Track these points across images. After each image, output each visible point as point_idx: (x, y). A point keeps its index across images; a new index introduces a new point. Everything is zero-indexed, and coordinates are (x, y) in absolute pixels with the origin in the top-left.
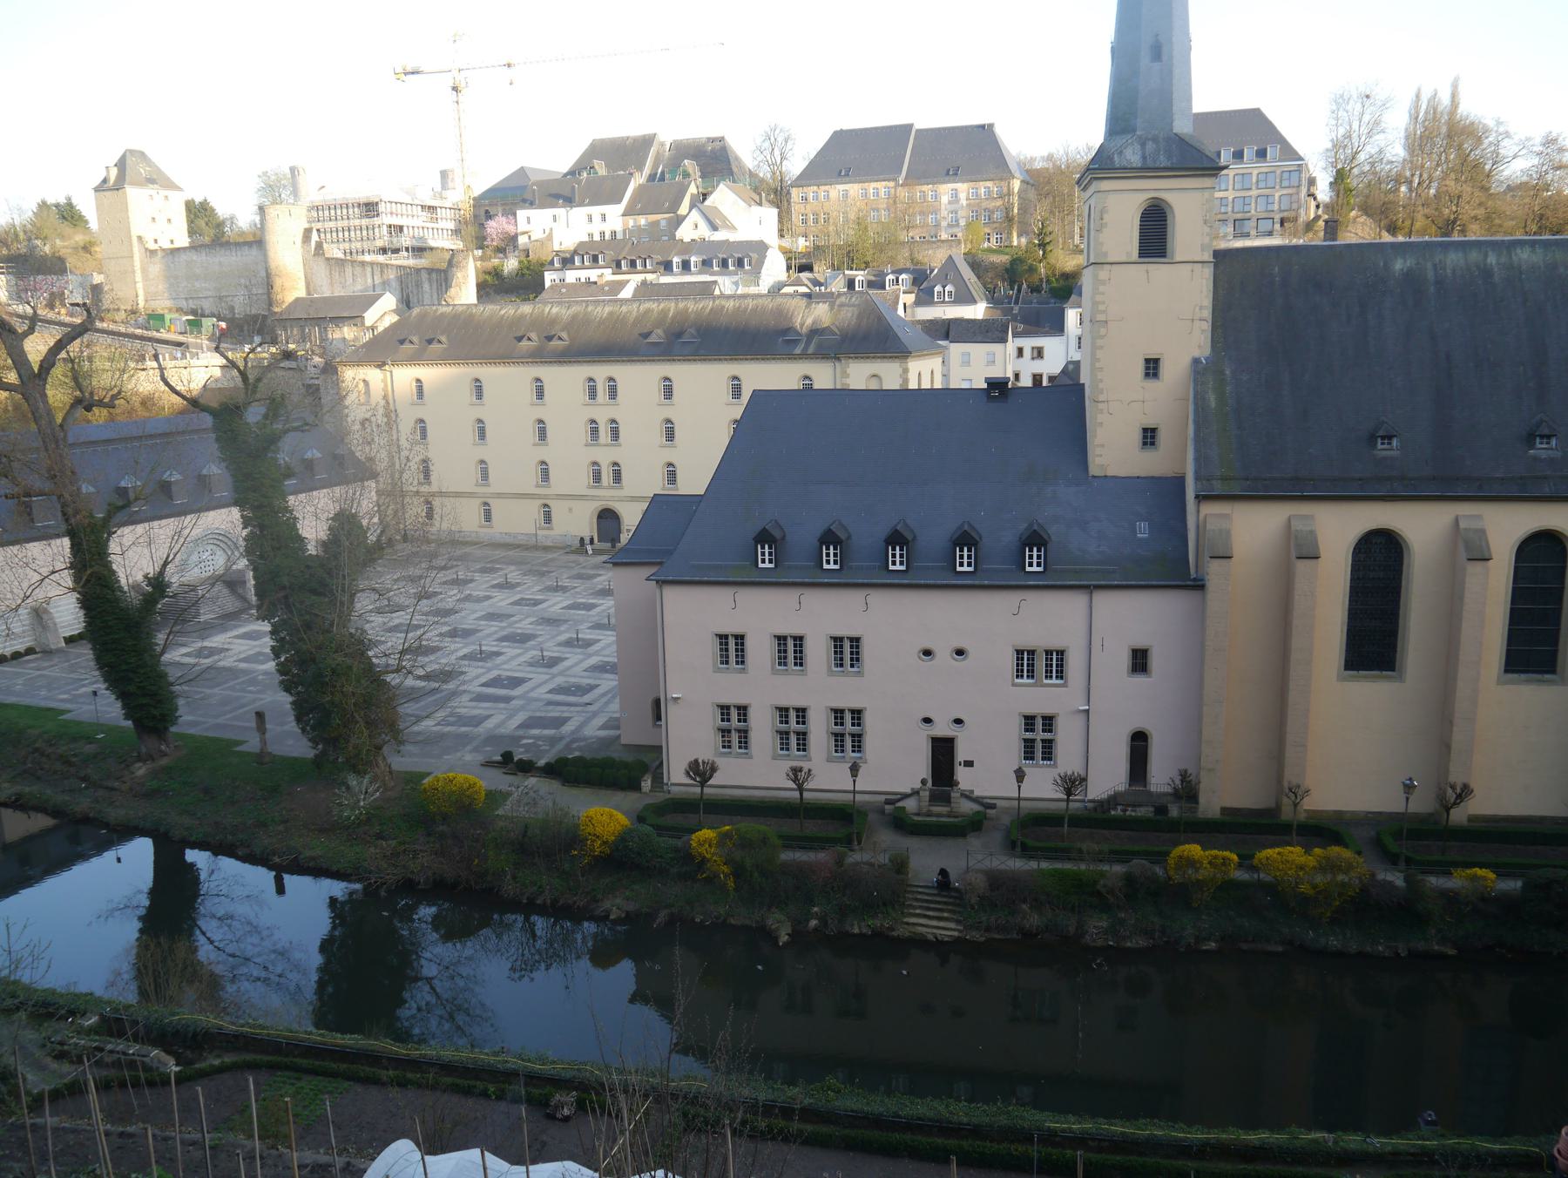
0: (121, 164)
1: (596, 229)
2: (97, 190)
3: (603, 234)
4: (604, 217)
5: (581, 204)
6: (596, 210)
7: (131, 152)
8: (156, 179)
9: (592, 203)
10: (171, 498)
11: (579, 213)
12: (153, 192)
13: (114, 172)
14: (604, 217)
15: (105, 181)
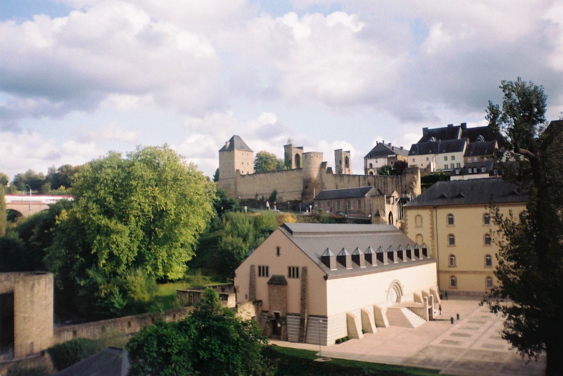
0: (232, 140)
1: (449, 162)
2: (220, 151)
3: (452, 165)
4: (453, 158)
5: (441, 152)
6: (449, 155)
7: (236, 136)
8: (245, 148)
9: (448, 151)
10: (393, 261)
11: (441, 156)
12: (243, 152)
13: (229, 144)
14: (453, 158)
15: (224, 147)
